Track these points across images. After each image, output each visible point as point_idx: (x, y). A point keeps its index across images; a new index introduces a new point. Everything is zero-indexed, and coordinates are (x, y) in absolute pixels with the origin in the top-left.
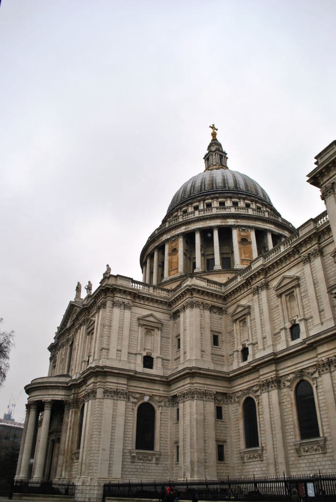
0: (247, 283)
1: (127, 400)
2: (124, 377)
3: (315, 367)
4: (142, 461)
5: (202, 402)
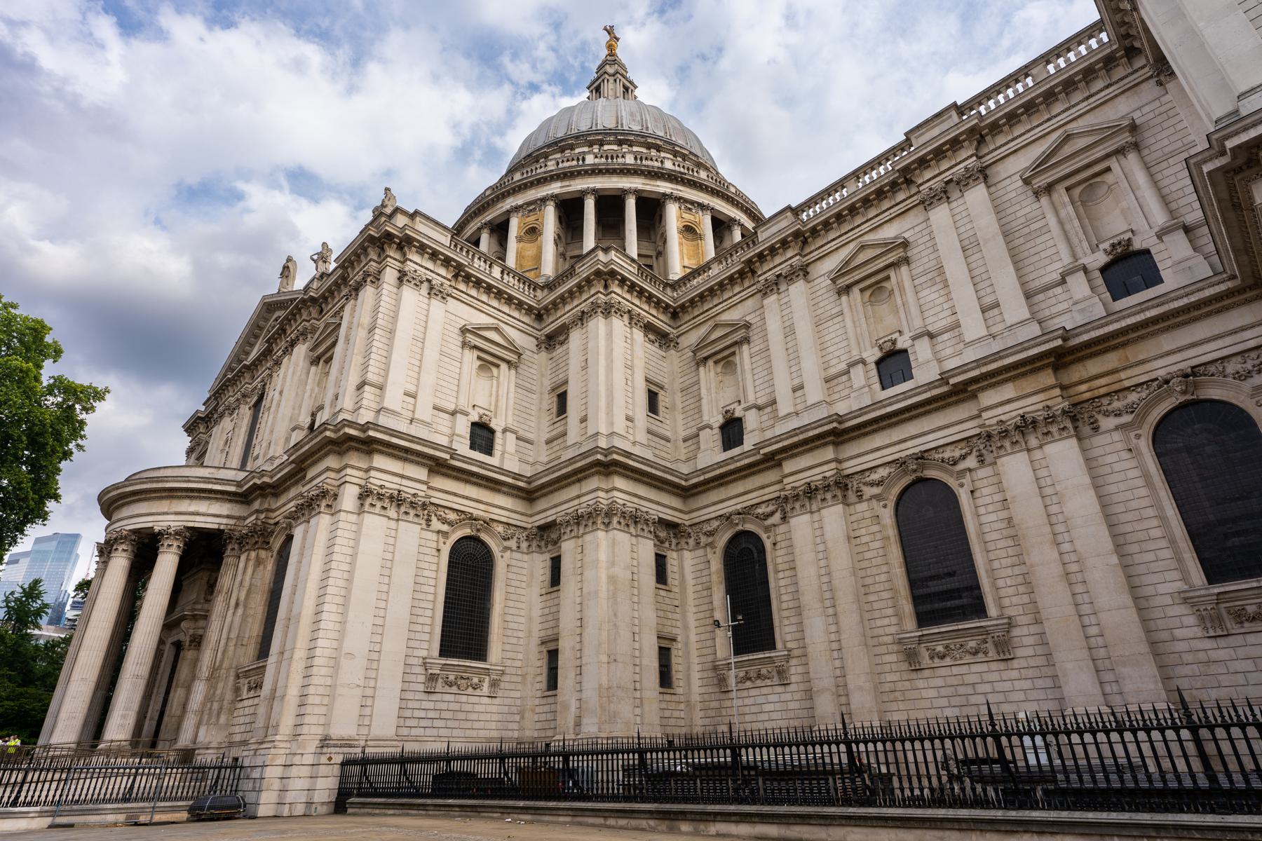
0: (748, 270)
1: (424, 522)
2: (418, 463)
3: (963, 444)
4: (454, 689)
5: (627, 536)
